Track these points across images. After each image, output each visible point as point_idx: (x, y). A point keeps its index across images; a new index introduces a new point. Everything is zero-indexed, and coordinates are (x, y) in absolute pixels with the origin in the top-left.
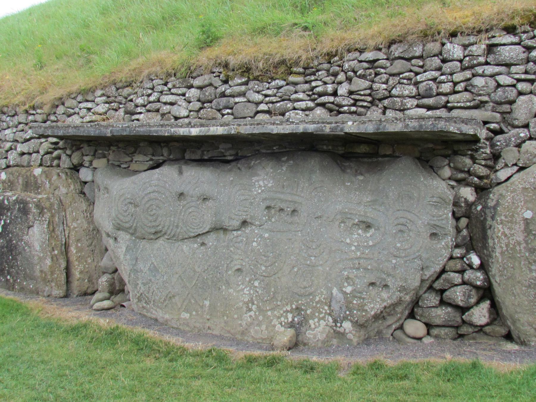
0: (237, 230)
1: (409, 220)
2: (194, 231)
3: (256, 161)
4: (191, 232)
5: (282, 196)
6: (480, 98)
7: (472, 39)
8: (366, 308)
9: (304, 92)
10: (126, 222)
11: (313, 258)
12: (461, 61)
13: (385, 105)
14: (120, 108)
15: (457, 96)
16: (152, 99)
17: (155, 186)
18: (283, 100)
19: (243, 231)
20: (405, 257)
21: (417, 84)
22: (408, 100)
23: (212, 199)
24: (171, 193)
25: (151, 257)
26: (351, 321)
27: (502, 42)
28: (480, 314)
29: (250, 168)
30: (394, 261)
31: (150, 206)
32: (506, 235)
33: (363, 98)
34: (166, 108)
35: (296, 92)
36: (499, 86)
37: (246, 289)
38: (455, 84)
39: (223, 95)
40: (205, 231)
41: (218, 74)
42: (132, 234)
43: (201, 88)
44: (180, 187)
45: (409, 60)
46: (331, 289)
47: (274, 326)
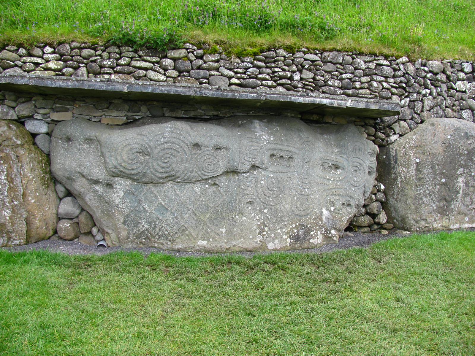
0: (248, 172)
1: (359, 163)
2: (208, 174)
3: (243, 121)
4: (205, 175)
5: (281, 147)
6: (375, 93)
7: (369, 59)
8: (342, 219)
9: (268, 74)
10: (133, 169)
11: (306, 190)
12: (363, 70)
13: (324, 90)
14: (80, 67)
15: (364, 91)
16: (122, 62)
17: (169, 137)
18: (251, 78)
19: (251, 173)
20: (359, 186)
21: (341, 80)
22: (338, 89)
23: (224, 148)
24: (186, 143)
25: (158, 198)
26: (335, 229)
27: (384, 64)
28: (383, 218)
29: (240, 126)
30: (353, 189)
31: (164, 155)
32: (404, 172)
33: (310, 84)
34: (142, 73)
35: (260, 73)
36: (383, 88)
37: (257, 217)
38: (362, 83)
39: (199, 68)
40: (218, 174)
41: (192, 50)
42: (134, 180)
43: (175, 60)
44: (195, 138)
45: (335, 64)
46: (321, 209)
47: (286, 240)
